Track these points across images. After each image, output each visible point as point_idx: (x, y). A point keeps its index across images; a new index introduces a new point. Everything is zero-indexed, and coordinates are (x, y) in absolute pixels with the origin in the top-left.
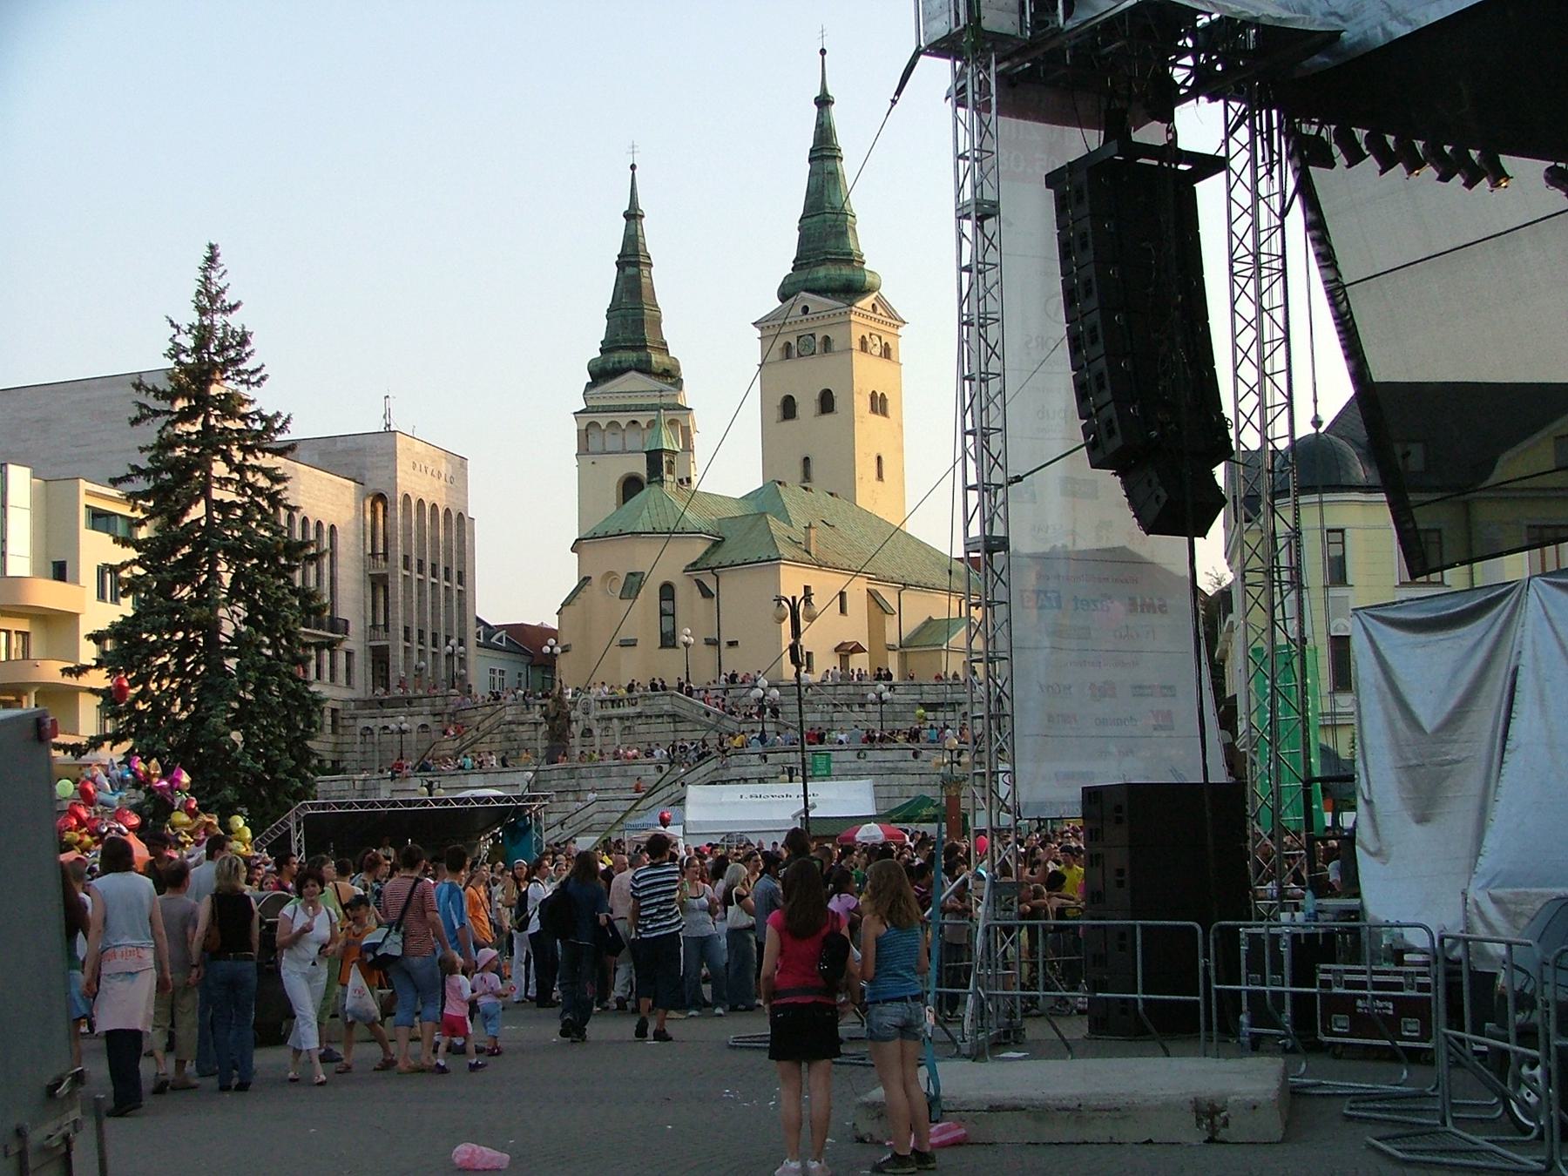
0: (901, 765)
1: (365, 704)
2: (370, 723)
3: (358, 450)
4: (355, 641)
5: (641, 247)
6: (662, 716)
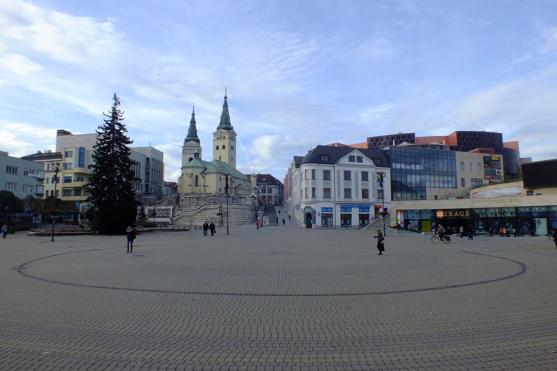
0: (238, 207)
1: (144, 194)
2: (145, 197)
4: (143, 183)
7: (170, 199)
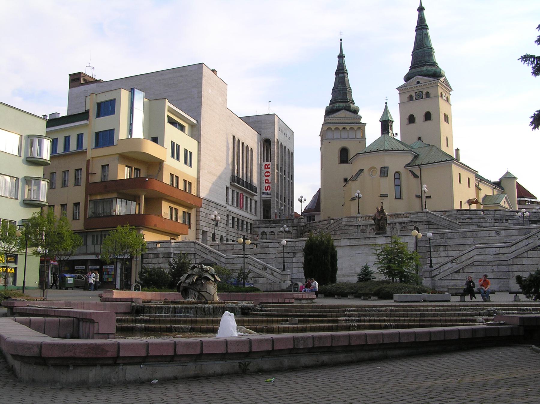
2: (265, 230)
3: (259, 121)
5: (344, 67)
6: (422, 222)
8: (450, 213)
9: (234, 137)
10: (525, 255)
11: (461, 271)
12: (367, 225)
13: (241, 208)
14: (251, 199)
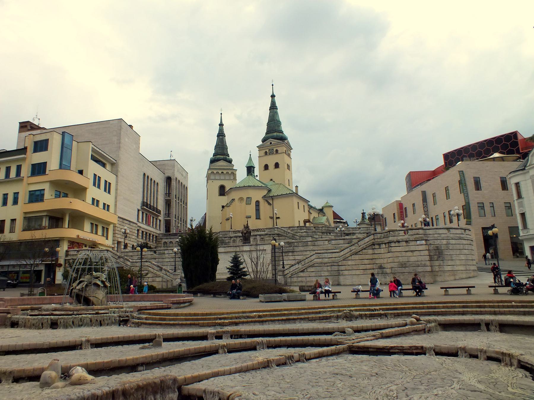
2: (166, 241)
3: (164, 165)
6: (275, 234)
7: (223, 238)
8: (293, 228)
9: (144, 174)
10: (350, 258)
11: (305, 271)
12: (236, 237)
13: (149, 225)
14: (156, 219)
